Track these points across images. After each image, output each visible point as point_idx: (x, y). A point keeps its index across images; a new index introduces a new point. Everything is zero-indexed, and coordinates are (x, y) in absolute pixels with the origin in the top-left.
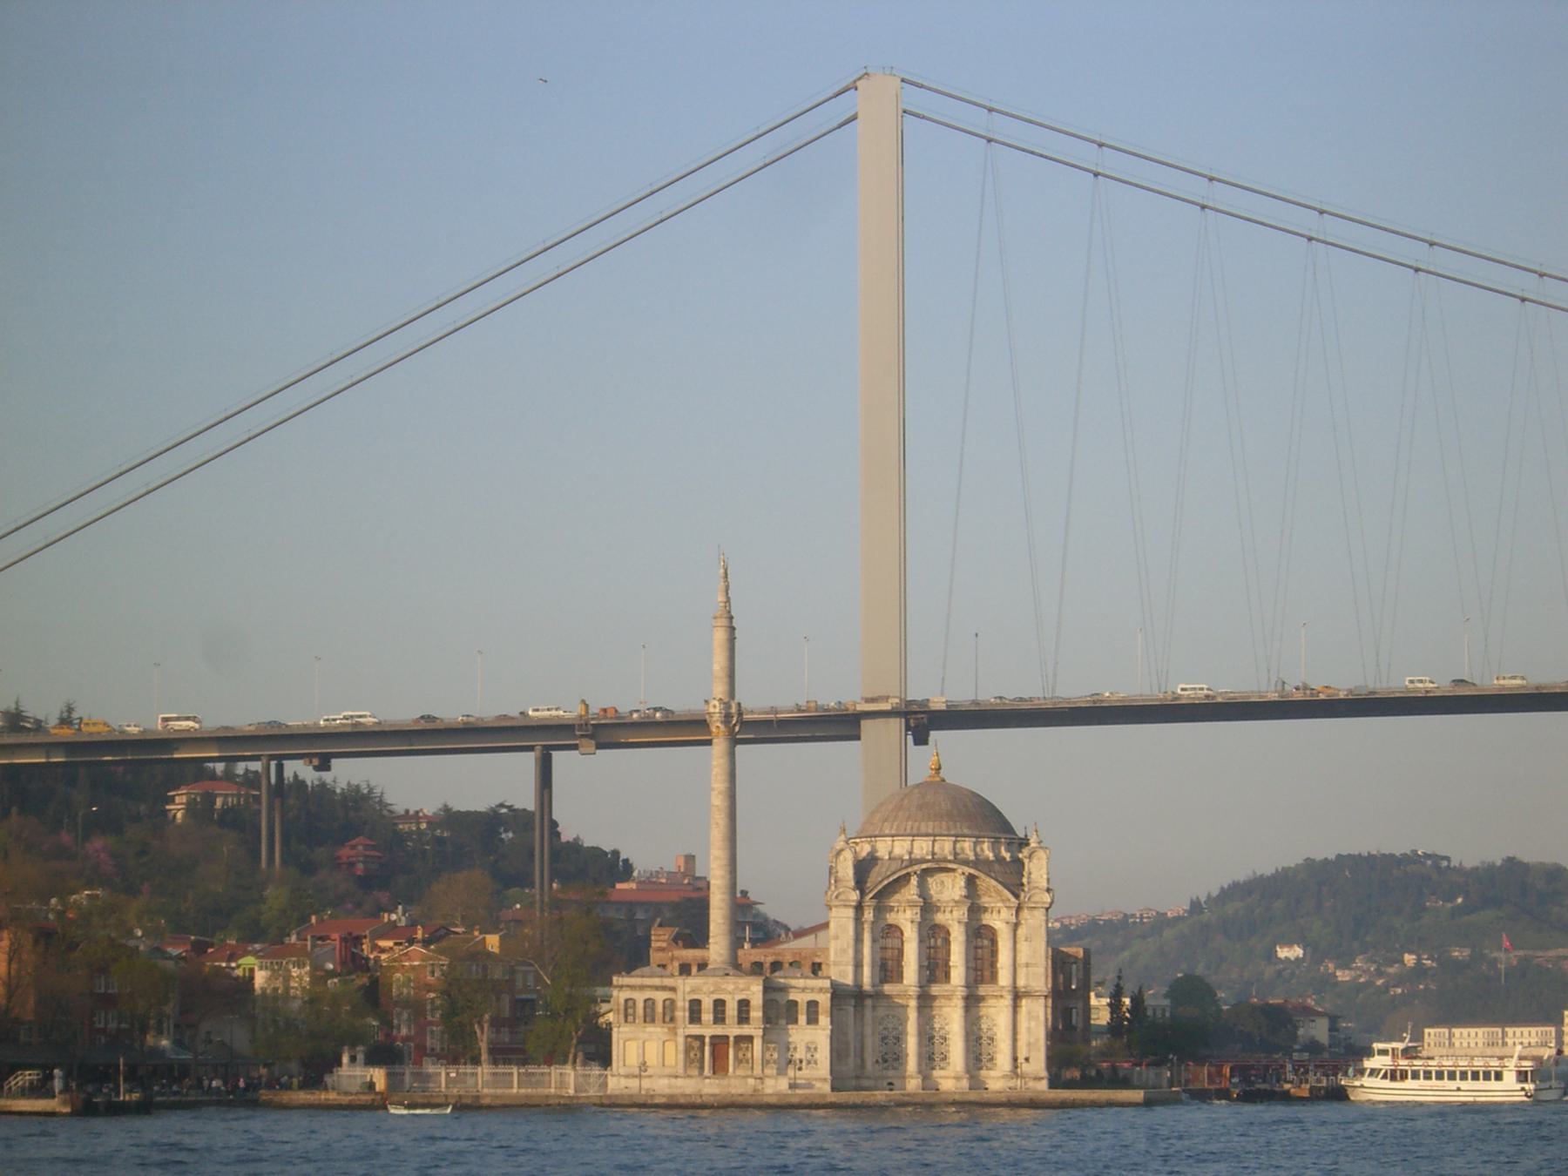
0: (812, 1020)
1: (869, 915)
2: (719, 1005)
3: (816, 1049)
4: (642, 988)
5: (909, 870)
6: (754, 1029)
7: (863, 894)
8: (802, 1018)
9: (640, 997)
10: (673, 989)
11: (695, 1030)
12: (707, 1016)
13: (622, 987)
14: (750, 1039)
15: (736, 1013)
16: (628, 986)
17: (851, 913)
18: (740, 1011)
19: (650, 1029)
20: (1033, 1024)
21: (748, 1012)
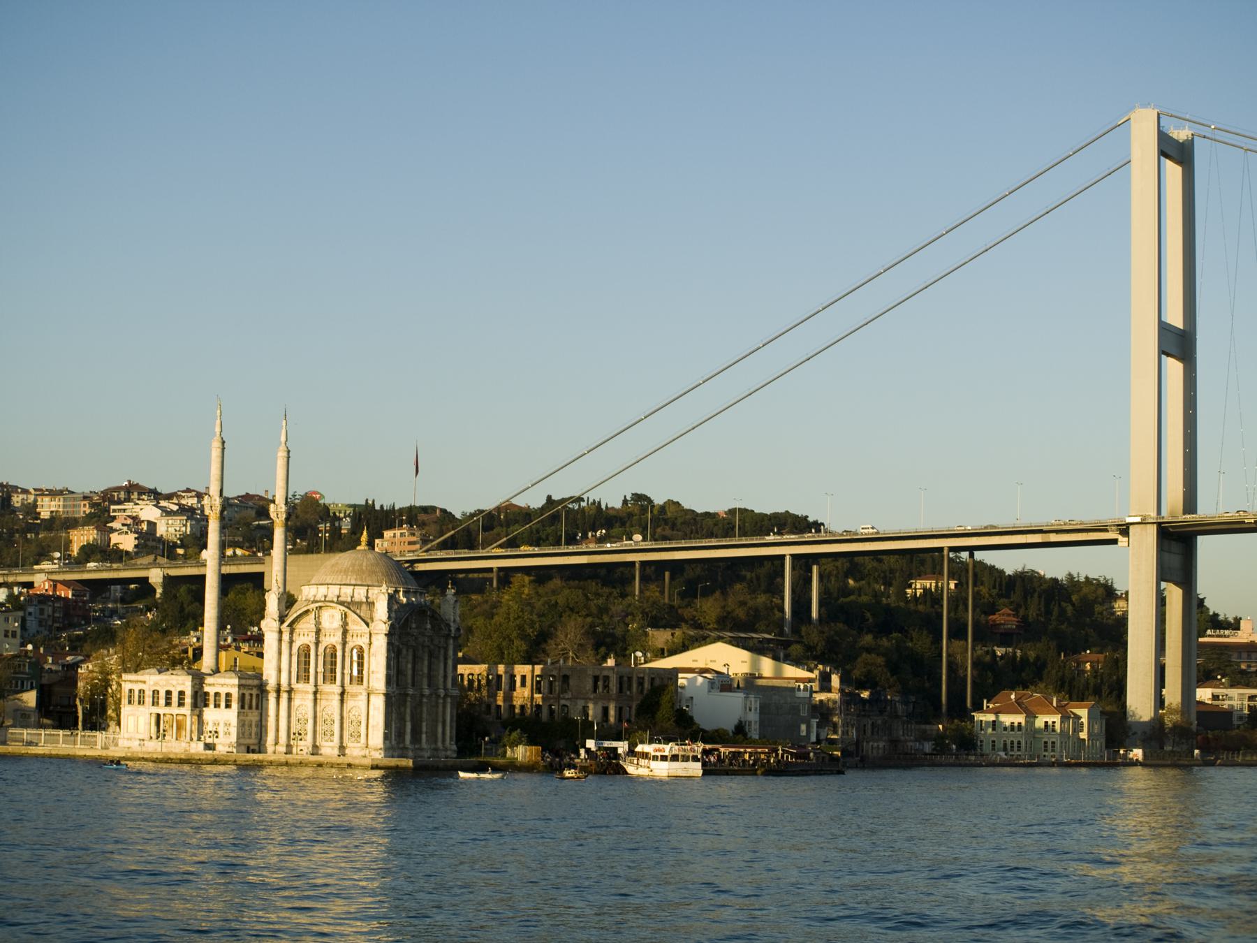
0: (228, 706)
1: (286, 637)
4: (137, 682)
5: (308, 607)
6: (186, 710)
9: (136, 687)
11: (156, 710)
12: (162, 701)
15: (177, 699)
16: (130, 681)
18: (180, 699)
19: (141, 708)
21: (184, 699)
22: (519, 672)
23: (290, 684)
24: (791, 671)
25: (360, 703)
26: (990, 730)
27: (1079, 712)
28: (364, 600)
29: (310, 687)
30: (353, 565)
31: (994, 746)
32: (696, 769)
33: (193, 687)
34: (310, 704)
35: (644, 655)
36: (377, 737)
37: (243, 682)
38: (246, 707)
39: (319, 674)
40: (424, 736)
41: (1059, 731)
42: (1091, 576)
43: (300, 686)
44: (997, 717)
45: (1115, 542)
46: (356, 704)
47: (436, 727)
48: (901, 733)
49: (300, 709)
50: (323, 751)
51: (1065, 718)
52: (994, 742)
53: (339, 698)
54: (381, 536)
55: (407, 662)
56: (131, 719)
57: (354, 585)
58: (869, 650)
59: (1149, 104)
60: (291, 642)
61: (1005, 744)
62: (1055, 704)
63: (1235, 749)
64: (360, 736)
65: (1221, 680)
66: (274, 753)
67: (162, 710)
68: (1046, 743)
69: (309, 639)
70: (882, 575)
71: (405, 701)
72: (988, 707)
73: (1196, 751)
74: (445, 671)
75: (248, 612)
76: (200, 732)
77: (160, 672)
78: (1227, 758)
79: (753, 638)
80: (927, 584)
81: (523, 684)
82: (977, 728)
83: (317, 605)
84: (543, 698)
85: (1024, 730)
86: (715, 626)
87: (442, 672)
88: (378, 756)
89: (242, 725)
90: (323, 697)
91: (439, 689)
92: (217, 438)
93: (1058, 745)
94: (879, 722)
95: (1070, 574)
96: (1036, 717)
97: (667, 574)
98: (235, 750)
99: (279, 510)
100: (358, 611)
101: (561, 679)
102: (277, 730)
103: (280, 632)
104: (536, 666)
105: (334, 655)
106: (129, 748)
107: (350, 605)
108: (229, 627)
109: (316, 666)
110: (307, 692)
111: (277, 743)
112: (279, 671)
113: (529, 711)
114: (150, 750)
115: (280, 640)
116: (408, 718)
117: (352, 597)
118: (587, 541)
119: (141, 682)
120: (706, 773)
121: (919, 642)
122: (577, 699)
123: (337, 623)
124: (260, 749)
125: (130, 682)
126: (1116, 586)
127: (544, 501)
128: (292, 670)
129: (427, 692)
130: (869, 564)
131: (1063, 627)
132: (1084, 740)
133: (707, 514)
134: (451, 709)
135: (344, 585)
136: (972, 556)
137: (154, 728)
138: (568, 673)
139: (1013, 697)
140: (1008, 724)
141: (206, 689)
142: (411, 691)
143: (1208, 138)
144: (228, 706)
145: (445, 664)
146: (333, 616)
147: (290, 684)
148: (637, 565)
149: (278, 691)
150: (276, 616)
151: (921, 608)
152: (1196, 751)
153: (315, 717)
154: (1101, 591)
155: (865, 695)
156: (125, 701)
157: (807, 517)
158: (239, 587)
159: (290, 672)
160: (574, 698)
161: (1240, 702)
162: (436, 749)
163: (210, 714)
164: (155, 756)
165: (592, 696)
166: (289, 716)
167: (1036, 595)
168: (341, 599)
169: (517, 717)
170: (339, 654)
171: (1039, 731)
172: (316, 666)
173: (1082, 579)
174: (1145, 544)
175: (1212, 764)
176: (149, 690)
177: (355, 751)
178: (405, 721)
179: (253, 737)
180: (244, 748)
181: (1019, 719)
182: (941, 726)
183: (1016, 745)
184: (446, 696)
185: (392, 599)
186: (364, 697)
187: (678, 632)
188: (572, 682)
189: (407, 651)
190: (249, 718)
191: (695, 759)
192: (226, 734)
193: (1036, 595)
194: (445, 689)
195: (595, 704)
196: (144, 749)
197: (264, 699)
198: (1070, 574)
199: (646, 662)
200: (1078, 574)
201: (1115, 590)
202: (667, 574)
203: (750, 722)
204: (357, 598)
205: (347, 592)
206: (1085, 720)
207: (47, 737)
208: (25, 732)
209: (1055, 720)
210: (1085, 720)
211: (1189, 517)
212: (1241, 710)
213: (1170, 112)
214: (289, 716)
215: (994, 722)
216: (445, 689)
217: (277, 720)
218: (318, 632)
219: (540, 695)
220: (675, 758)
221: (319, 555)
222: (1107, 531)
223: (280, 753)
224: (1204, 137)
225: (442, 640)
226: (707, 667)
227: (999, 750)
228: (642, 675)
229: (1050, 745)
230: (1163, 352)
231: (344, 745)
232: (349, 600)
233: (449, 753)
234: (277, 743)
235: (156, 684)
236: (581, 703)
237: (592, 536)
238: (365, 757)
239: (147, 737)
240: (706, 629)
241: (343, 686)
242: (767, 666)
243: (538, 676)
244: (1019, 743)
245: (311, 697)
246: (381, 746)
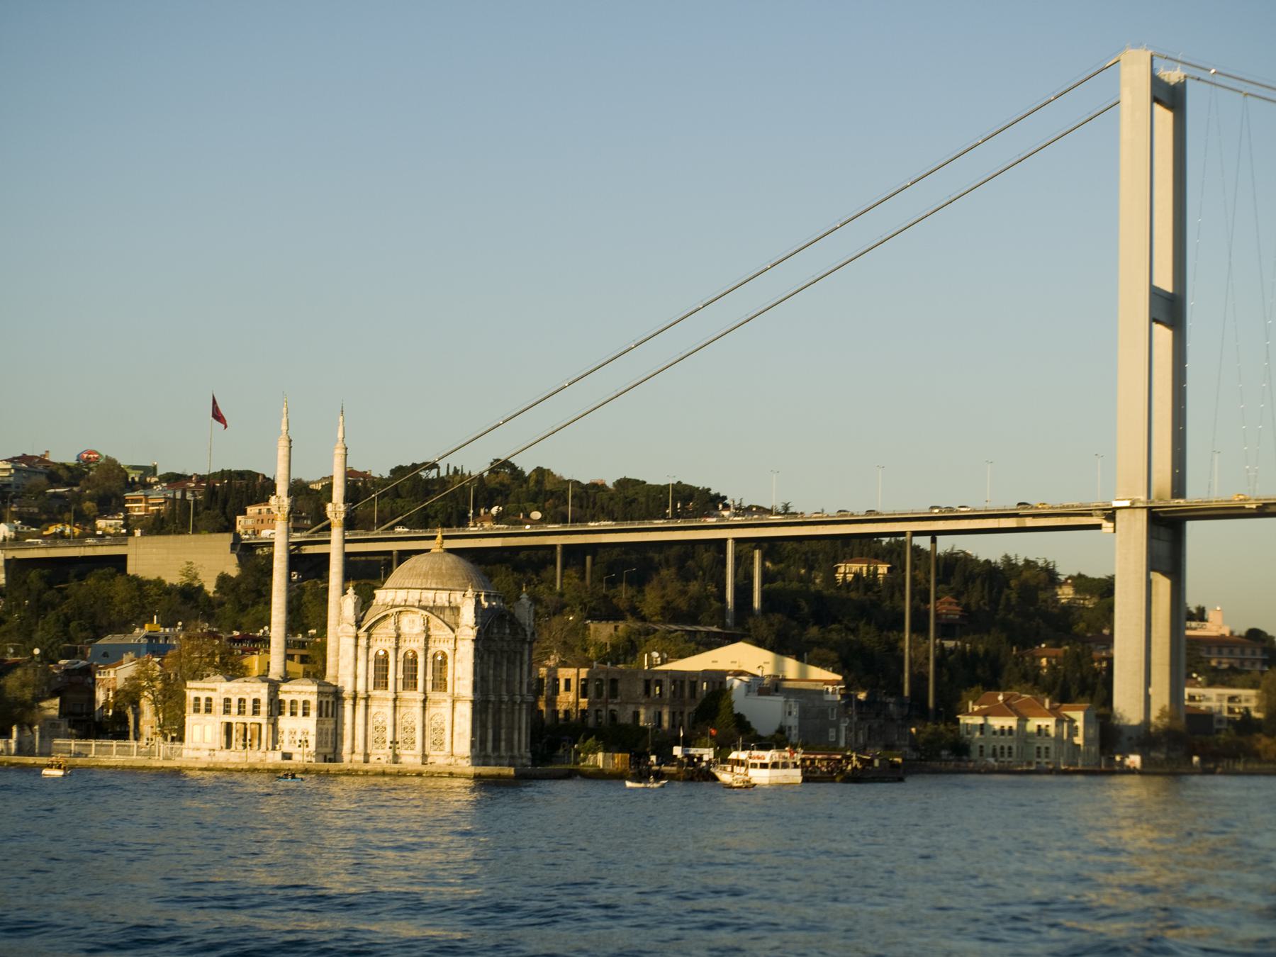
0: (305, 714)
3: (307, 733)
4: (203, 689)
6: (262, 718)
7: (359, 627)
9: (203, 696)
10: (214, 690)
11: (227, 719)
12: (234, 710)
13: (191, 689)
15: (251, 708)
18: (254, 707)
19: (208, 717)
21: (259, 707)
22: (563, 675)
23: (367, 691)
24: (817, 673)
25: (444, 710)
26: (978, 734)
27: (1073, 714)
28: (447, 604)
29: (390, 694)
30: (432, 568)
31: (981, 752)
32: (795, 775)
33: (269, 694)
34: (389, 711)
35: (661, 656)
36: (463, 744)
37: (321, 689)
38: (324, 714)
39: (398, 681)
40: (503, 744)
41: (1053, 735)
42: (1031, 558)
43: (378, 693)
44: (986, 720)
45: (1098, 527)
46: (440, 711)
47: (512, 733)
48: (896, 737)
49: (378, 716)
50: (402, 759)
51: (1060, 722)
52: (981, 747)
53: (421, 705)
54: (244, 513)
55: (489, 668)
56: (197, 729)
57: (437, 589)
58: (819, 644)
59: (1141, 44)
60: (368, 648)
61: (994, 750)
62: (1047, 705)
63: (1235, 757)
64: (414, 743)
65: (1196, 678)
66: (351, 762)
67: (234, 718)
68: (1039, 748)
69: (389, 645)
70: (803, 557)
71: (487, 708)
72: (973, 709)
73: (1196, 759)
74: (521, 678)
75: (117, 600)
76: (275, 741)
77: (229, 680)
78: (1228, 765)
79: (700, 631)
80: (855, 567)
81: (568, 688)
82: (963, 731)
83: (398, 609)
84: (589, 703)
85: (1015, 734)
86: (660, 618)
87: (518, 678)
88: (467, 767)
89: (320, 733)
90: (404, 704)
91: (514, 695)
92: (284, 436)
93: (1052, 750)
94: (876, 726)
95: (1006, 556)
96: (1027, 720)
97: (589, 558)
98: (313, 760)
99: (337, 509)
100: (442, 616)
101: (609, 683)
102: (353, 739)
103: (357, 637)
104: (581, 670)
105: (414, 661)
106: (197, 758)
107: (433, 609)
108: (180, 623)
109: (395, 672)
110: (387, 700)
111: (353, 752)
112: (356, 677)
113: (574, 716)
114: (221, 760)
115: (356, 646)
116: (490, 725)
117: (434, 602)
118: (479, 519)
119: (208, 689)
120: (806, 780)
121: (867, 636)
122: (627, 703)
123: (418, 628)
124: (335, 756)
125: (194, 690)
126: (1058, 570)
128: (369, 676)
129: (506, 698)
130: (789, 546)
131: (1011, 616)
132: (1079, 745)
133: (594, 486)
134: (527, 715)
135: (425, 589)
136: (934, 541)
137: (224, 739)
138: (616, 676)
139: (1001, 698)
140: (997, 727)
141: (281, 696)
142: (492, 698)
143: (1203, 80)
144: (305, 714)
145: (521, 669)
146: (413, 621)
147: (367, 691)
148: (559, 549)
149: (355, 698)
150: (352, 621)
151: (853, 595)
152: (1196, 759)
153: (395, 725)
154: (1043, 575)
155: (862, 696)
156: (189, 709)
157: (709, 489)
158: (101, 571)
159: (367, 679)
160: (624, 704)
161: (1218, 704)
162: (512, 757)
163: (285, 722)
164: (240, 767)
165: (643, 701)
166: (366, 724)
167: (978, 581)
168: (423, 603)
169: (561, 722)
170: (421, 660)
171: (1031, 735)
172: (395, 672)
173: (1021, 563)
174: (1134, 529)
175: (1211, 772)
176: (220, 698)
177: (439, 760)
178: (487, 729)
179: (330, 745)
180: (321, 757)
181: (1010, 722)
182: (913, 730)
183: (1006, 751)
184: (522, 702)
185: (478, 603)
186: (449, 704)
187: (622, 625)
188: (621, 686)
189: (489, 657)
190: (325, 726)
191: (796, 766)
193: (978, 581)
194: (521, 695)
195: (647, 708)
196: (214, 759)
197: (340, 707)
198: (1006, 556)
199: (662, 663)
200: (1016, 556)
201: (1058, 574)
202: (589, 558)
203: (790, 728)
204: (439, 603)
205: (428, 597)
206: (1080, 724)
207: (98, 748)
208: (73, 742)
209: (1049, 723)
210: (1080, 724)
211: (1182, 502)
212: (1220, 712)
213: (1166, 54)
214: (366, 724)
215: (982, 725)
216: (521, 695)
217: (354, 728)
218: (398, 637)
219: (586, 700)
220: (775, 766)
221: (187, 536)
222: (1091, 515)
223: (357, 762)
224: (1198, 79)
225: (518, 645)
226: (741, 669)
227: (988, 756)
228: (695, 679)
229: (1043, 751)
230: (1154, 319)
231: (427, 753)
232: (431, 604)
233: (524, 761)
234: (353, 752)
235: (227, 691)
236: (631, 709)
237: (485, 513)
238: (450, 765)
239: (217, 746)
240: (650, 622)
241: (425, 693)
242: (791, 667)
243: (583, 680)
244: (1010, 748)
245: (391, 704)
246: (469, 754)
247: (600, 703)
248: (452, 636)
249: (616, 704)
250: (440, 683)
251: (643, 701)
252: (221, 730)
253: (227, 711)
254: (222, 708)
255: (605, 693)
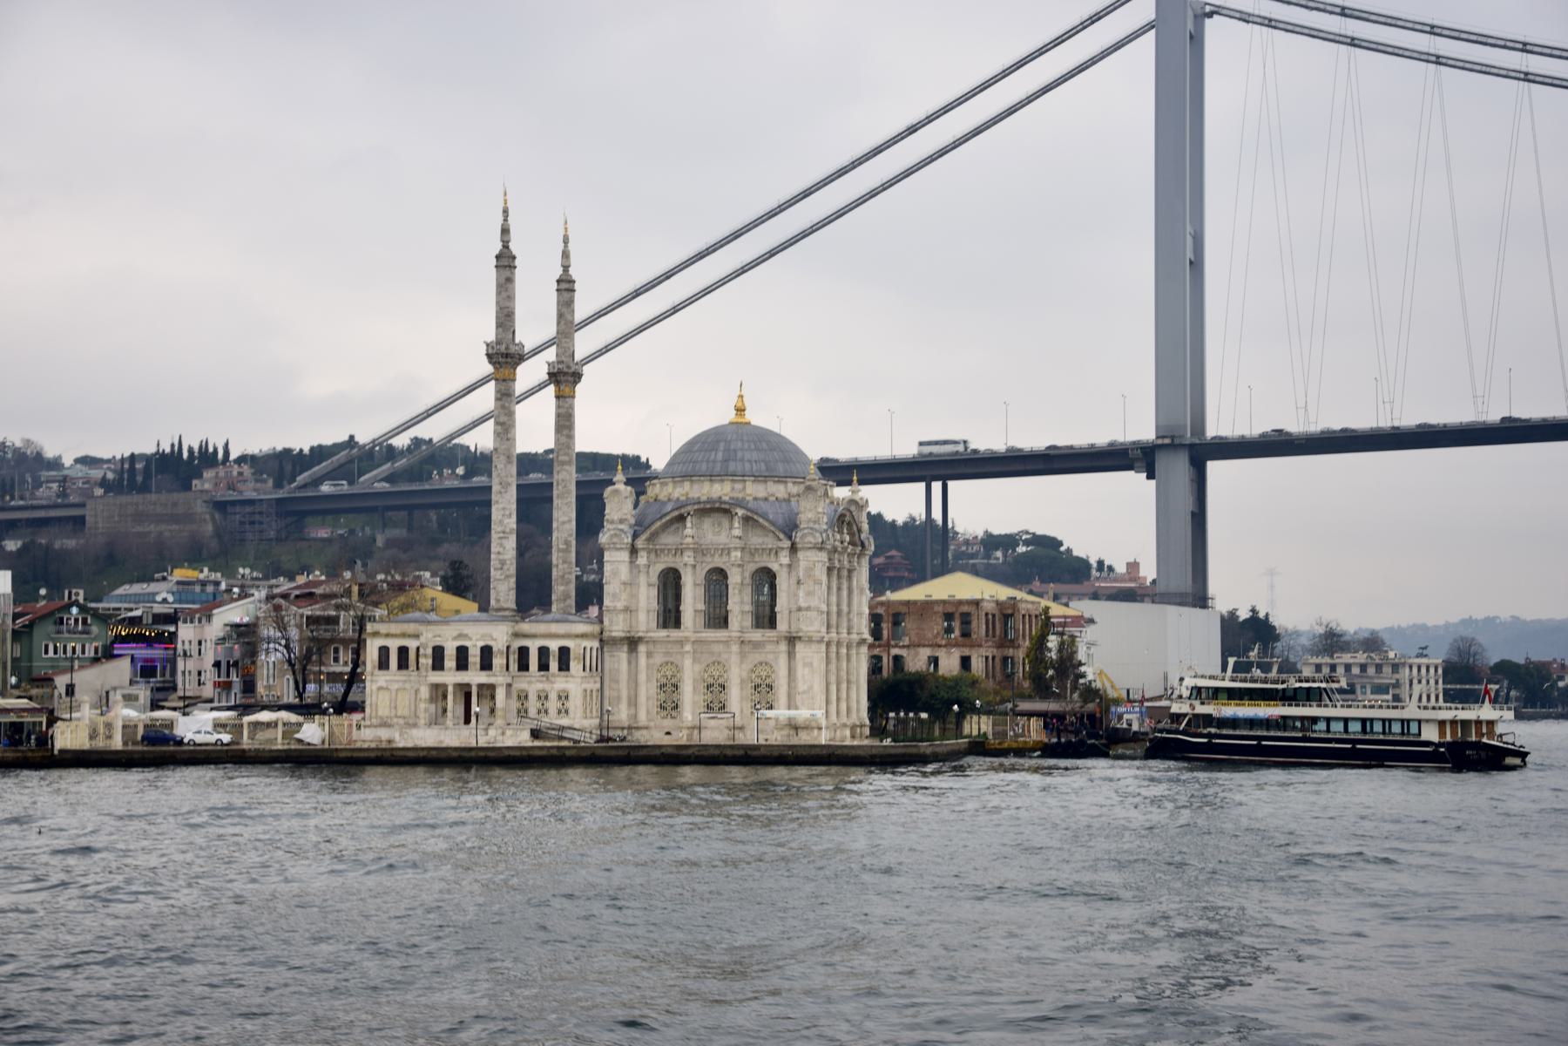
0: (564, 666)
2: (462, 653)
3: (567, 697)
8: (554, 665)
9: (394, 645)
11: (437, 677)
12: (450, 663)
14: (492, 687)
17: (624, 556)
20: (806, 671)
54: (200, 476)
101: (891, 619)
122: (919, 646)
127: (346, 438)
192: (560, 712)
236: (925, 653)
247: (879, 646)
248: (787, 544)
249: (904, 647)
250: (766, 618)
251: (944, 642)
252: (425, 692)
253: (438, 664)
254: (430, 661)
255: (885, 633)
